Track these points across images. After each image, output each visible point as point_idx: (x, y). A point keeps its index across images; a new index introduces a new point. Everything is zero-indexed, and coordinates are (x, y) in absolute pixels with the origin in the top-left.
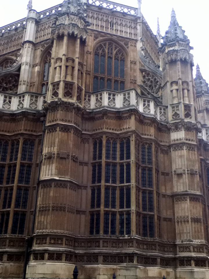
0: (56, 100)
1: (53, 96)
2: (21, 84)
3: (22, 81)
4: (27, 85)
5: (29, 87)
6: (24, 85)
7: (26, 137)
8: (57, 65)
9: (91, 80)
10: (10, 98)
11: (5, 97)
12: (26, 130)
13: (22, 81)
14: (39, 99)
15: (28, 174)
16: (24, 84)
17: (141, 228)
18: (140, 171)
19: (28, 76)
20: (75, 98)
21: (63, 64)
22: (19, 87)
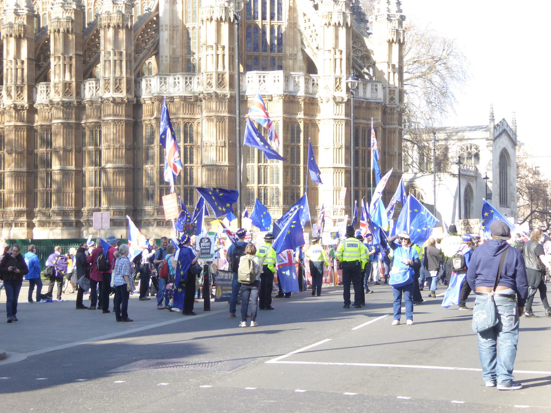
0: (211, 92)
1: (208, 86)
2: (162, 30)
3: (164, 26)
4: (170, 30)
5: (171, 32)
6: (166, 31)
7: (186, 121)
8: (208, 53)
9: (243, 32)
10: (165, 79)
11: (161, 78)
12: (185, 114)
13: (164, 26)
14: (192, 80)
15: (192, 154)
16: (166, 29)
17: (289, 198)
18: (289, 149)
19: (170, 18)
20: (227, 88)
21: (214, 52)
22: (161, 33)
